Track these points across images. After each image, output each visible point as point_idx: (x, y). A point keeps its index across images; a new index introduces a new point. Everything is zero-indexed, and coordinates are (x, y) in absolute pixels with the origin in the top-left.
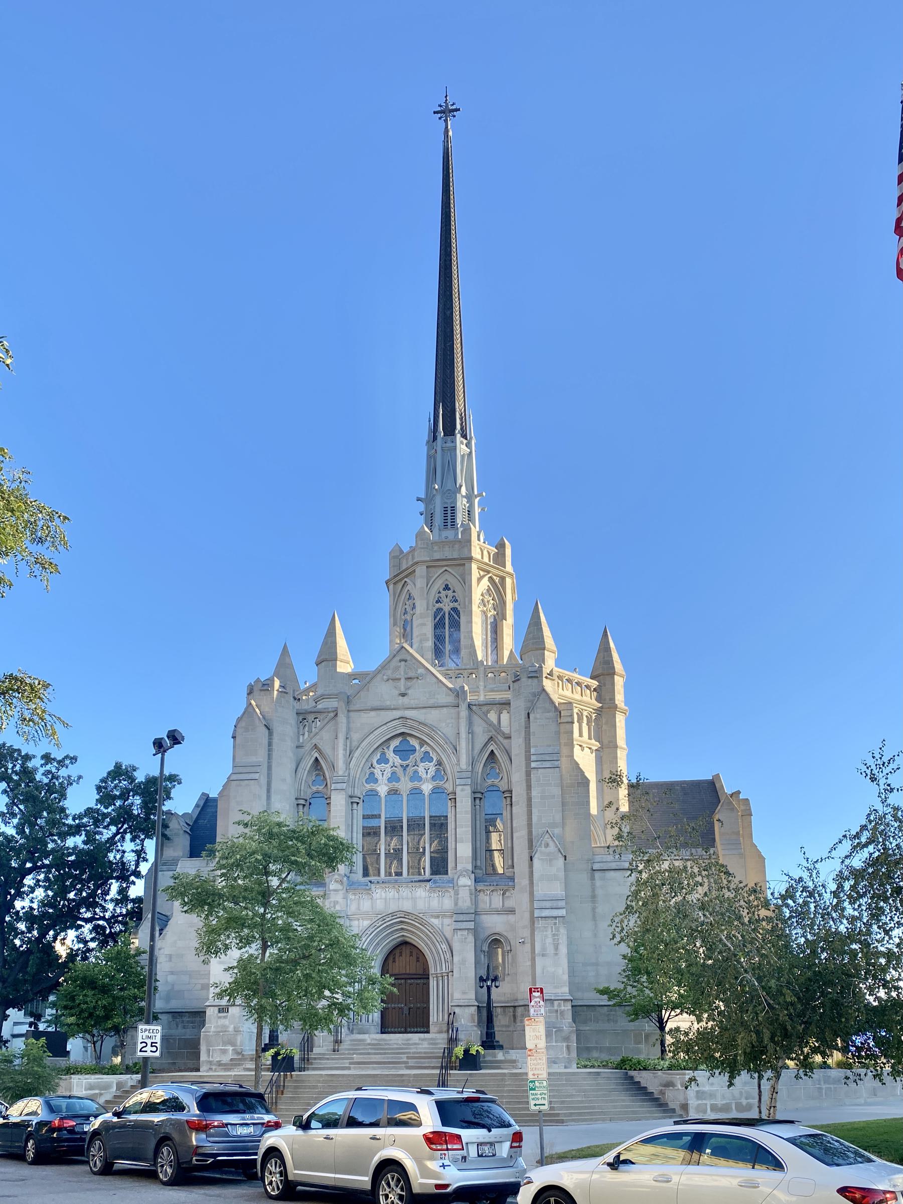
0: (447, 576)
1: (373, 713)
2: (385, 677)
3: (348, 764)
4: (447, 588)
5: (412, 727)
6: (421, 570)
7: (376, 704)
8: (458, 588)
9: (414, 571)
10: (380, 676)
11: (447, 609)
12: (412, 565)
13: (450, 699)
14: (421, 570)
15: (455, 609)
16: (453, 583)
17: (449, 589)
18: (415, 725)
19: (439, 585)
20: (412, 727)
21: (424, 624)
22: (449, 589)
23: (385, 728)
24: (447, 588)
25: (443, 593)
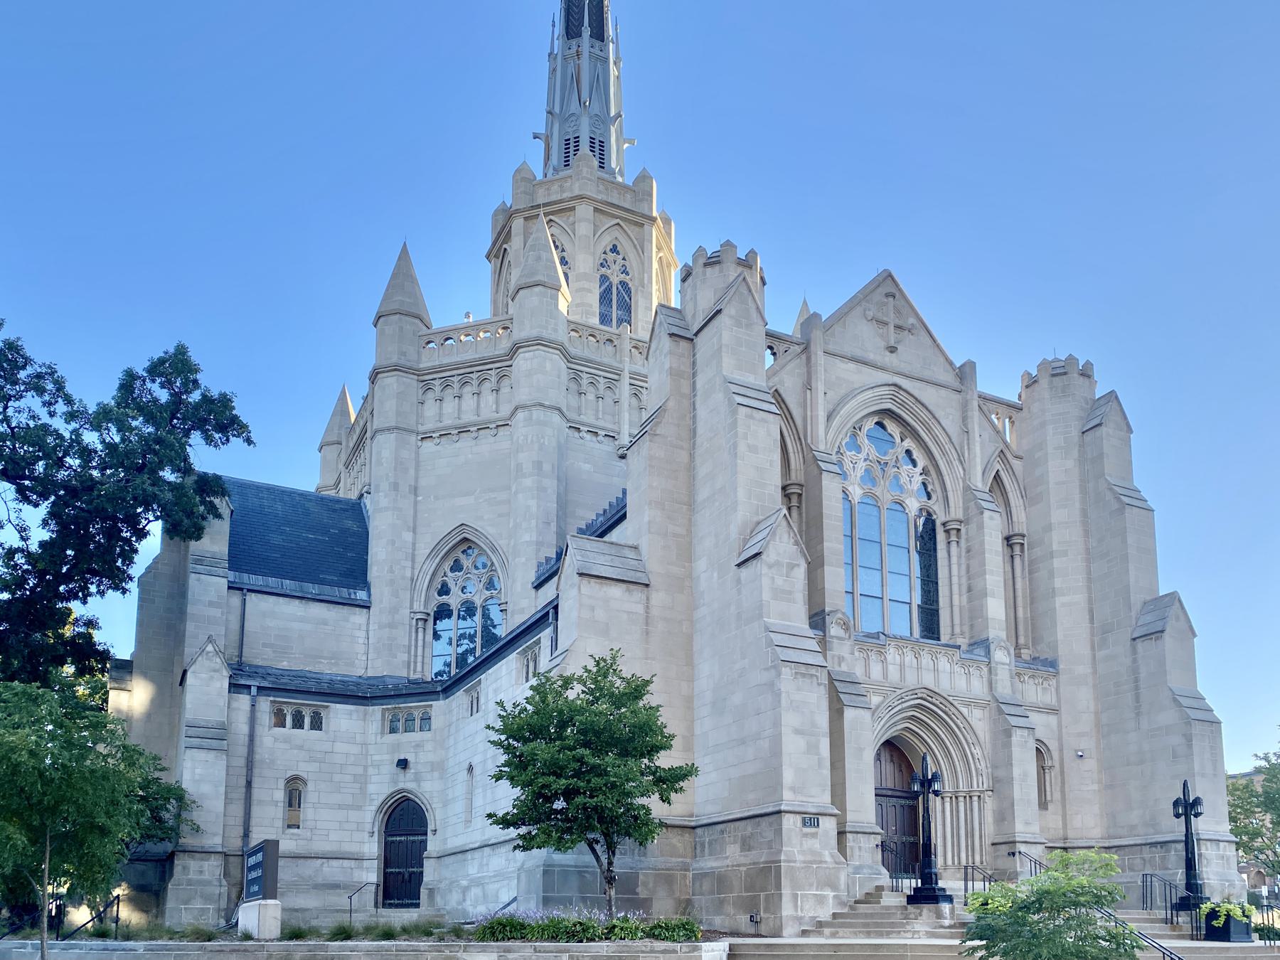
0: (616, 233)
1: (852, 366)
2: (870, 314)
3: (826, 435)
4: (614, 249)
5: (902, 405)
6: (584, 210)
7: (858, 353)
8: (632, 255)
9: (573, 208)
10: (859, 310)
11: (615, 280)
12: (572, 199)
13: (948, 378)
14: (584, 210)
15: (623, 283)
16: (625, 246)
17: (618, 253)
18: (910, 402)
19: (606, 241)
20: (902, 405)
21: (590, 291)
22: (618, 253)
23: (869, 394)
24: (614, 249)
25: (611, 256)
